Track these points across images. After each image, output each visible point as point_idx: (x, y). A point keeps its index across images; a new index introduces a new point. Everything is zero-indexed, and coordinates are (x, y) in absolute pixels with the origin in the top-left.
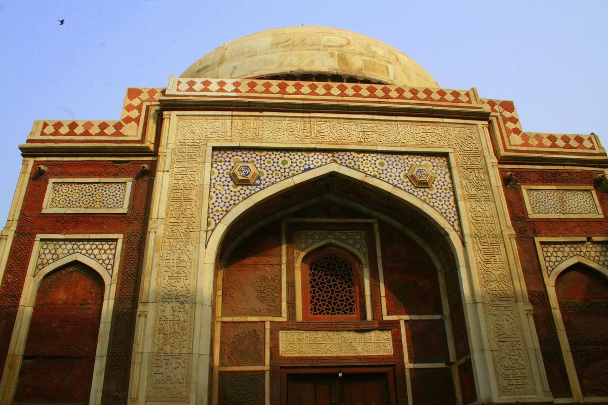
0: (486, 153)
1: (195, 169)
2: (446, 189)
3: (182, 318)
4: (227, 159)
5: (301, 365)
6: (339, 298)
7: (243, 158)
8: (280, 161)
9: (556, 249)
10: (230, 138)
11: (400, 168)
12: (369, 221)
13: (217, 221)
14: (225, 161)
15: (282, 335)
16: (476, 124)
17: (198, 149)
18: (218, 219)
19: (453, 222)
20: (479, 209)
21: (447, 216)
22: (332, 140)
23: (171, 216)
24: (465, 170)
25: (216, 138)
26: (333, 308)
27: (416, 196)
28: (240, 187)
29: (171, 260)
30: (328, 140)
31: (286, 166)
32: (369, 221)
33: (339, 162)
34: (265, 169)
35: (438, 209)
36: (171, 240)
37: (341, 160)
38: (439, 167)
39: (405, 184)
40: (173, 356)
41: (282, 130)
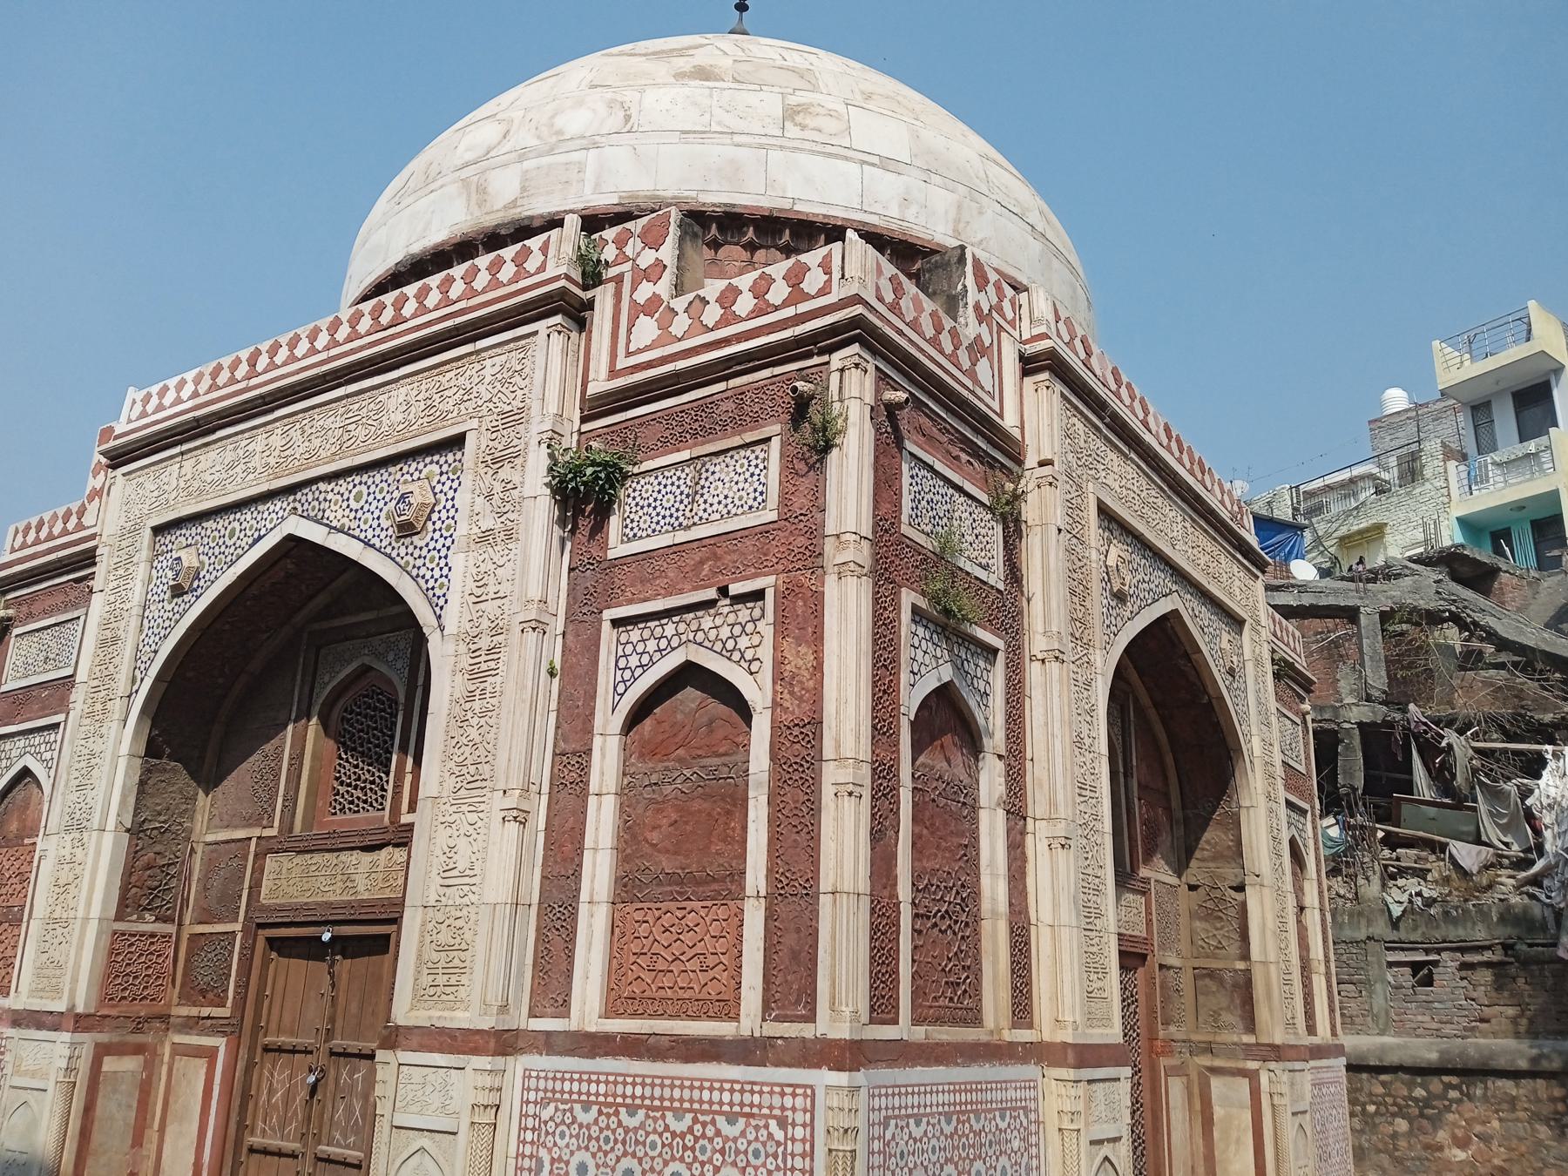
5: (280, 920)
9: (647, 633)
15: (270, 863)
16: (536, 333)
27: (393, 559)
28: (175, 600)
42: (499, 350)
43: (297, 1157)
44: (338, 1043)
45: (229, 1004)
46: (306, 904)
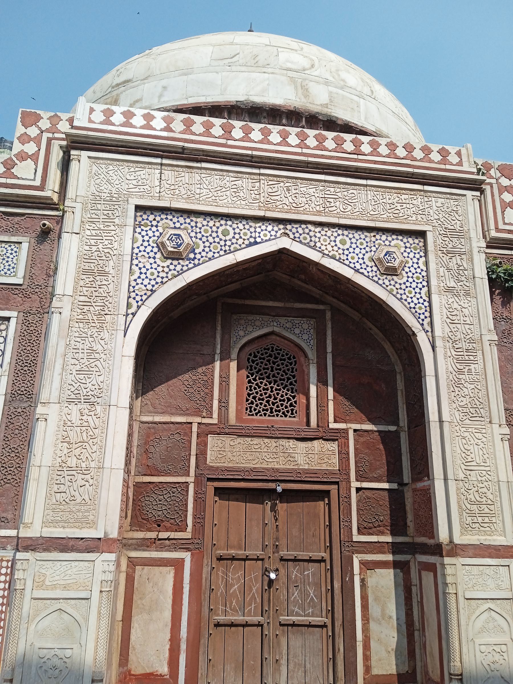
0: (473, 234)
1: (113, 233)
2: (418, 278)
3: (92, 425)
4: (154, 223)
6: (279, 397)
7: (174, 223)
8: (220, 231)
10: (158, 195)
11: (365, 249)
12: (321, 307)
13: (140, 303)
14: (152, 226)
16: (465, 195)
17: (116, 207)
18: (142, 300)
19: (423, 320)
20: (455, 305)
21: (416, 312)
22: (286, 207)
23: (82, 294)
24: (444, 255)
25: (141, 194)
26: (271, 409)
27: (381, 285)
28: (169, 261)
29: (80, 349)
30: (281, 207)
31: (228, 238)
32: (321, 307)
33: (292, 236)
34: (201, 239)
35: (406, 303)
36: (81, 325)
37: (294, 234)
38: (412, 250)
39: (369, 269)
40: (79, 471)
41: (224, 189)
42: (440, 196)
43: (262, 626)
44: (283, 553)
45: (190, 528)
46: (255, 468)
